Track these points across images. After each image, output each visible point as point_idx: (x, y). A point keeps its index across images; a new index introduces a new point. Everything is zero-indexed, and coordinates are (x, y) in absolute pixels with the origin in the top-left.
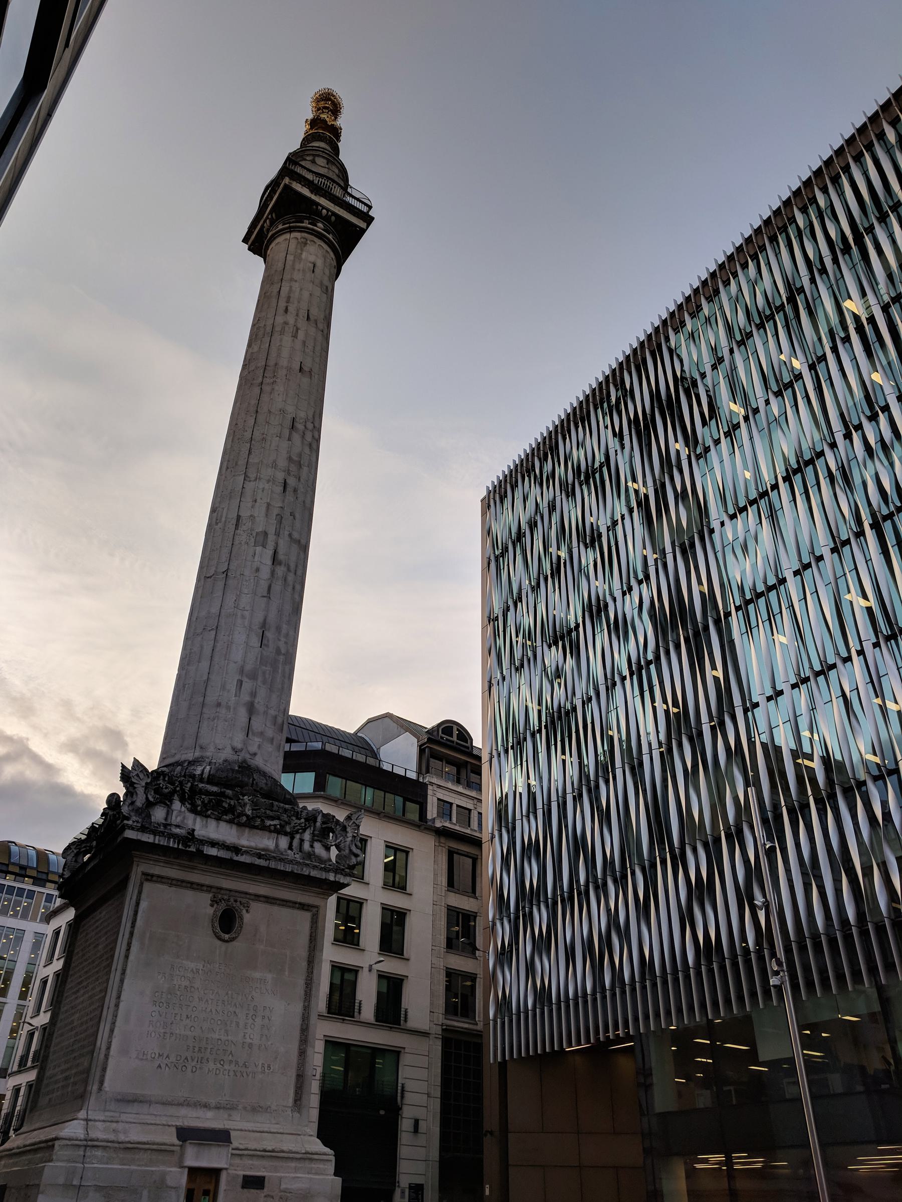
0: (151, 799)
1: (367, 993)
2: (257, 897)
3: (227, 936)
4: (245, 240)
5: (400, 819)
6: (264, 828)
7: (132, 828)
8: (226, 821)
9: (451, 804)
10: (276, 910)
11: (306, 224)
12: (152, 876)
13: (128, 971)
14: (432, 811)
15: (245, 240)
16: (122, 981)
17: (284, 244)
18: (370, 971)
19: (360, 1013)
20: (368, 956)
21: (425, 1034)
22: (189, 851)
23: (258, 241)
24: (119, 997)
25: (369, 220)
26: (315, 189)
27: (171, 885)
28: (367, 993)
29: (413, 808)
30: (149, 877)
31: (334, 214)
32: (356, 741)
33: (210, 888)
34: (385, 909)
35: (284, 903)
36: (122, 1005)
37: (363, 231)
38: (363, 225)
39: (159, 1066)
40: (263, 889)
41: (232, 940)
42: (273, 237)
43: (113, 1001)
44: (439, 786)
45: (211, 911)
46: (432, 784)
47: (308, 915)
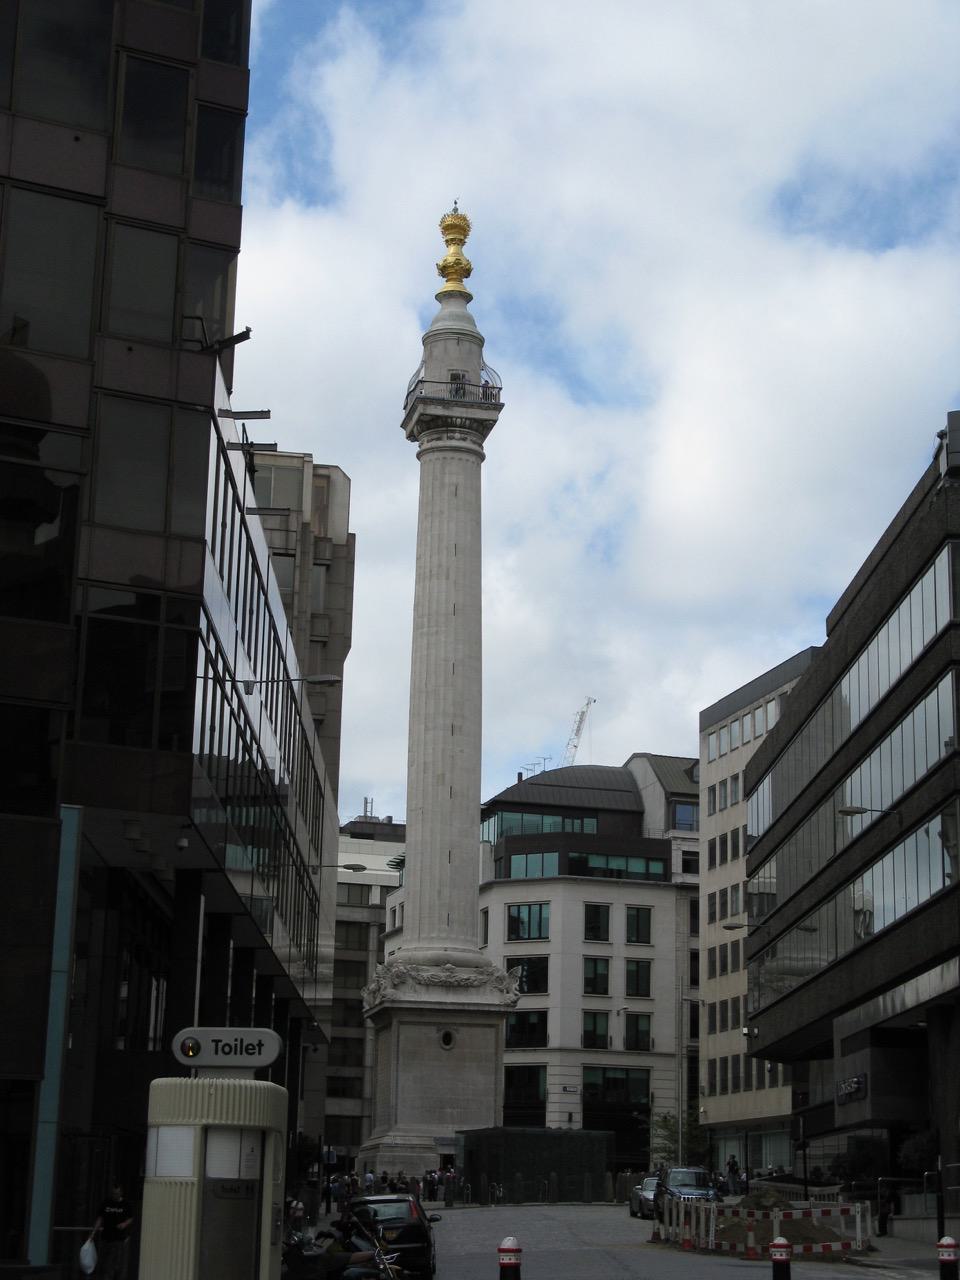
1: (617, 1031)
3: (448, 1047)
7: (388, 1001)
15: (404, 425)
18: (618, 1014)
20: (617, 1000)
21: (672, 1055)
28: (617, 1031)
29: (656, 868)
30: (401, 1023)
31: (466, 419)
34: (629, 961)
40: (465, 1021)
41: (452, 1048)
44: (684, 839)
45: (437, 1035)
46: (675, 838)
47: (493, 1029)
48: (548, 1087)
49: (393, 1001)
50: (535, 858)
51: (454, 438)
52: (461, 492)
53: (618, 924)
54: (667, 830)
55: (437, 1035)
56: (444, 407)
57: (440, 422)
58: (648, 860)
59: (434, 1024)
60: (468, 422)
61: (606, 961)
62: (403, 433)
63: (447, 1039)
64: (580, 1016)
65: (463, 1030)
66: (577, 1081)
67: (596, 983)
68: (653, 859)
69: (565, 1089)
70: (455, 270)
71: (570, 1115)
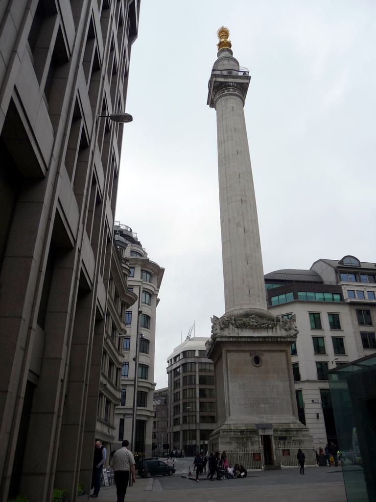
0: (222, 327)
2: (265, 351)
3: (258, 365)
4: (207, 104)
5: (333, 302)
6: (261, 328)
7: (218, 337)
8: (249, 328)
9: (354, 291)
10: (272, 354)
11: (226, 92)
12: (229, 350)
13: (229, 380)
14: (346, 295)
16: (228, 384)
17: (220, 102)
19: (331, 378)
22: (237, 342)
23: (212, 103)
24: (228, 389)
25: (249, 78)
26: (225, 77)
27: (235, 352)
29: (337, 297)
30: (228, 351)
32: (312, 272)
33: (248, 351)
35: (274, 351)
36: (230, 391)
37: (248, 84)
38: (246, 81)
39: (246, 407)
41: (260, 366)
42: (216, 102)
43: (227, 390)
44: (347, 285)
46: (343, 285)
47: (284, 353)
48: (304, 400)
49: (222, 337)
50: (282, 297)
51: (230, 91)
52: (235, 109)
53: (325, 321)
54: (338, 282)
55: (250, 358)
56: (225, 79)
57: (223, 85)
58: (333, 294)
59: (248, 351)
60: (235, 84)
61: (322, 338)
62: (209, 106)
63: (257, 360)
64: (315, 364)
65: (265, 354)
66: (318, 397)
67: (319, 349)
68: (335, 294)
69: (313, 401)
70: (225, 46)
71: (318, 414)
